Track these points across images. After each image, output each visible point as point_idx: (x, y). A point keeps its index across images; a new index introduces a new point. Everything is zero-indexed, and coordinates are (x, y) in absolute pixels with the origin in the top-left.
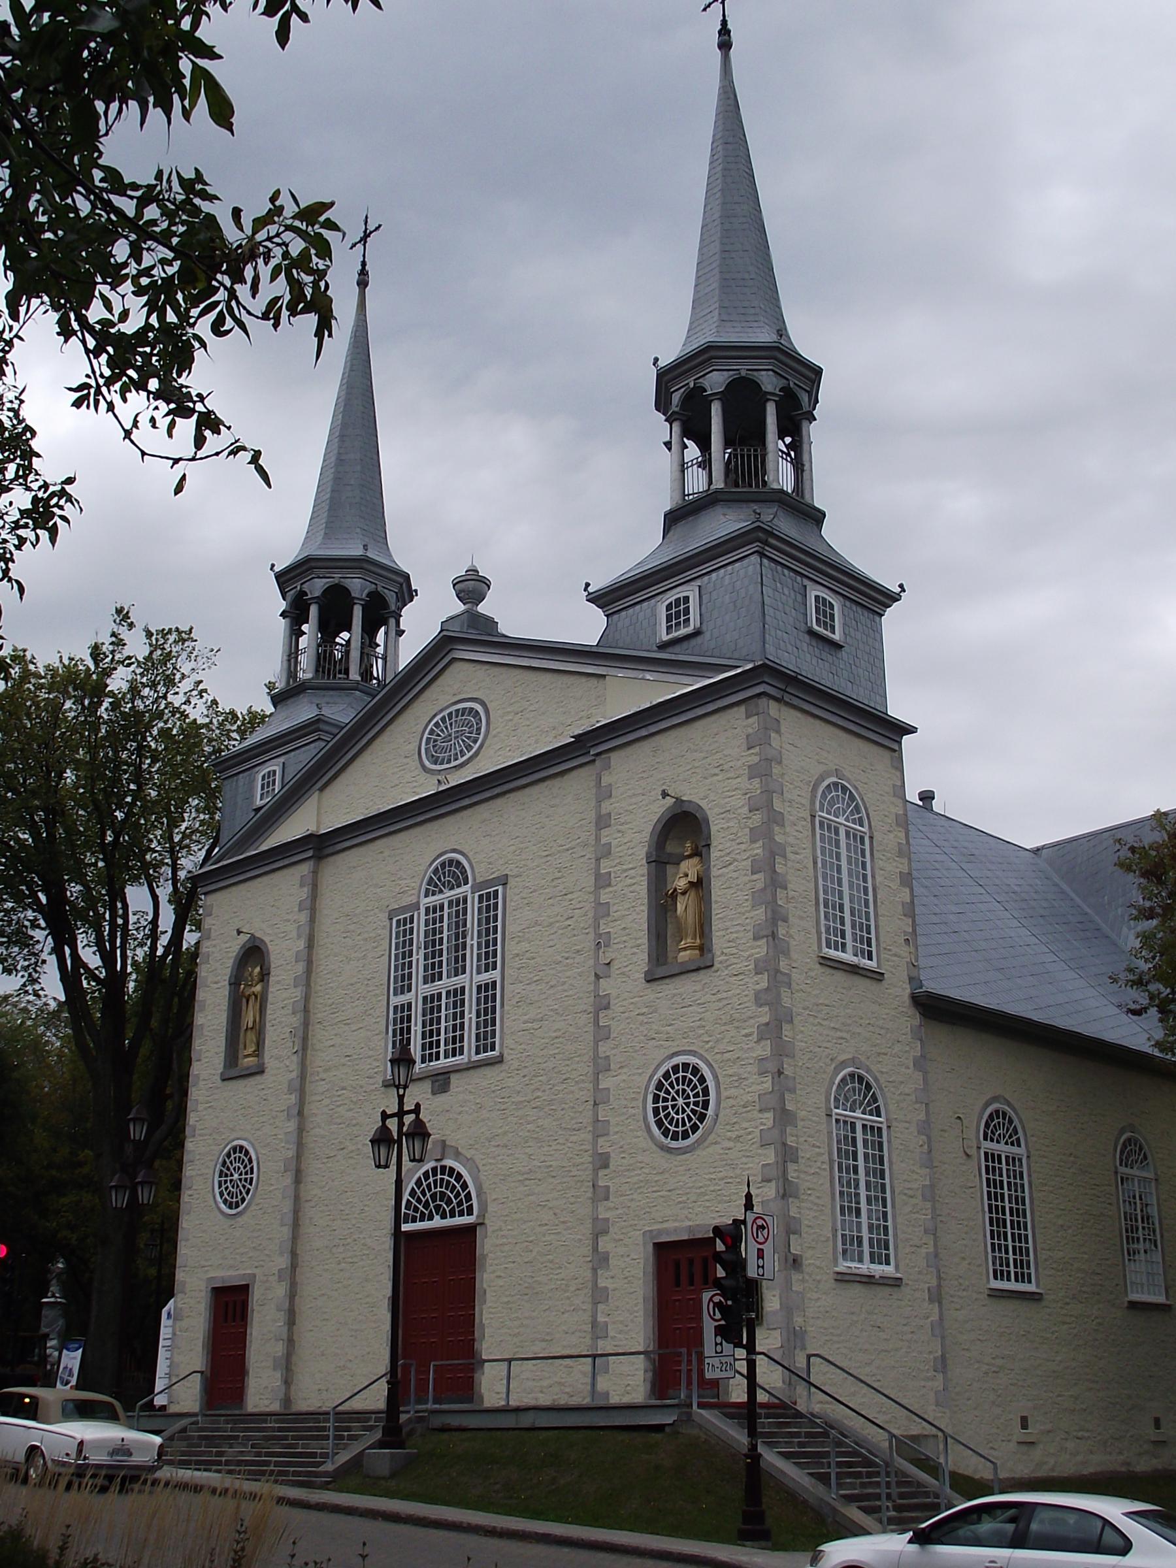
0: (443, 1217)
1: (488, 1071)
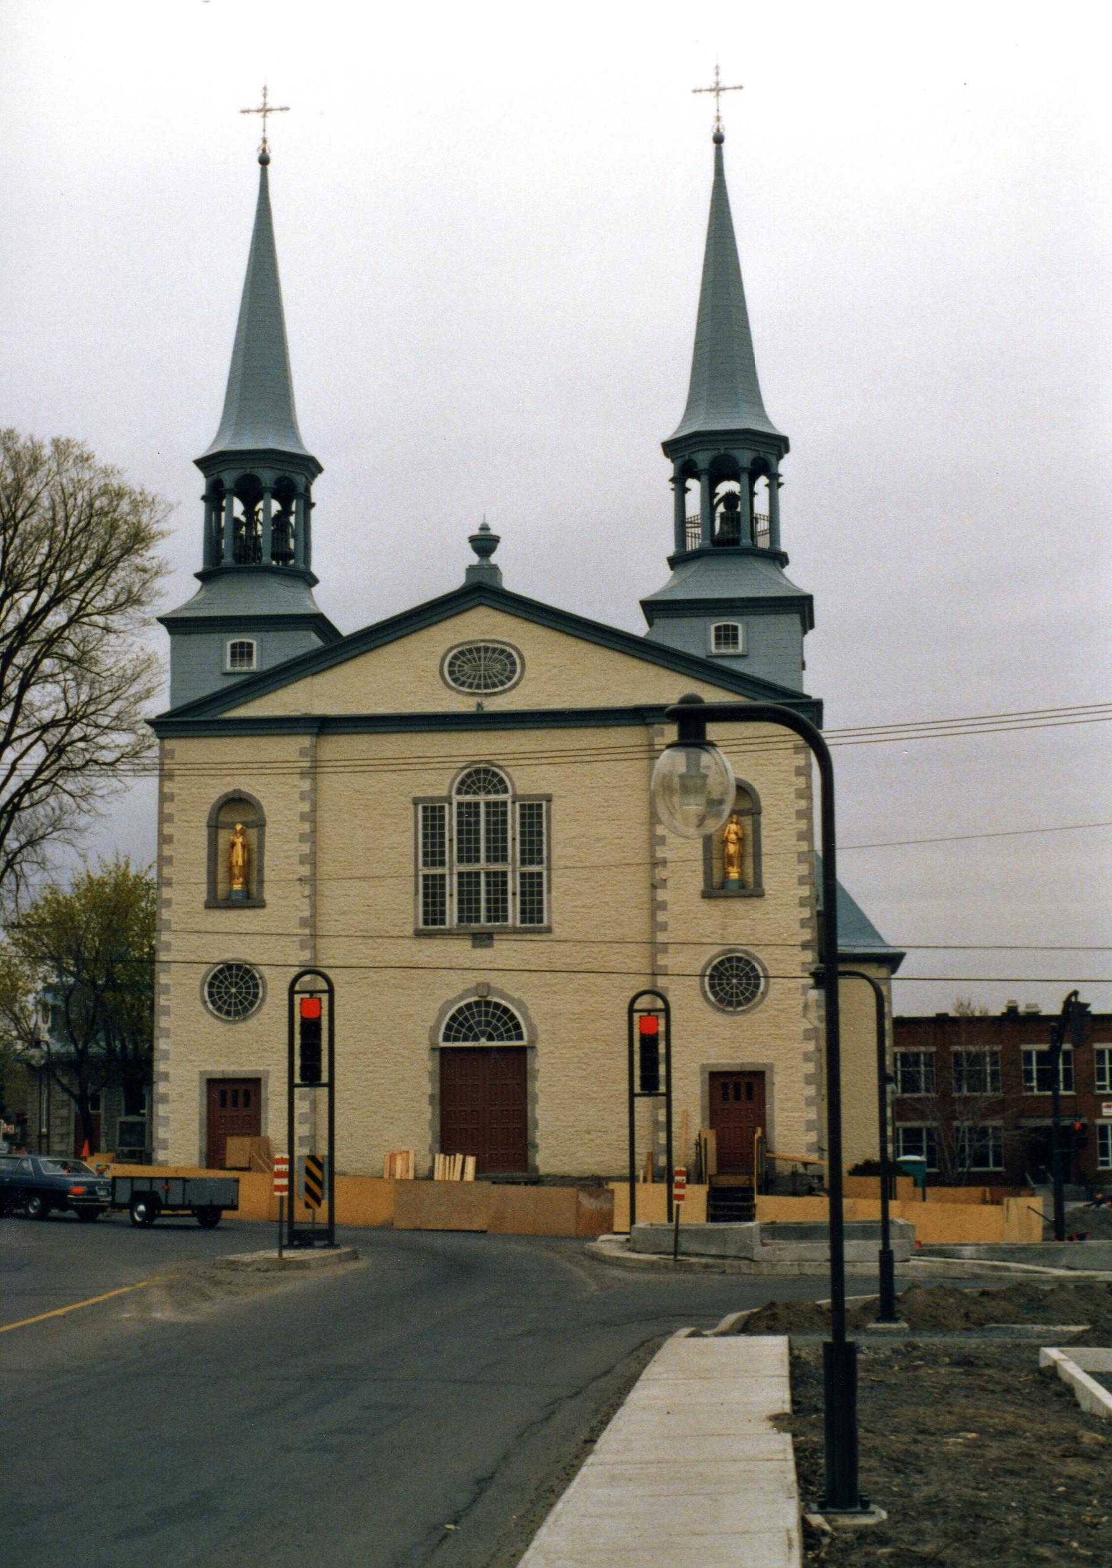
0: (490, 1038)
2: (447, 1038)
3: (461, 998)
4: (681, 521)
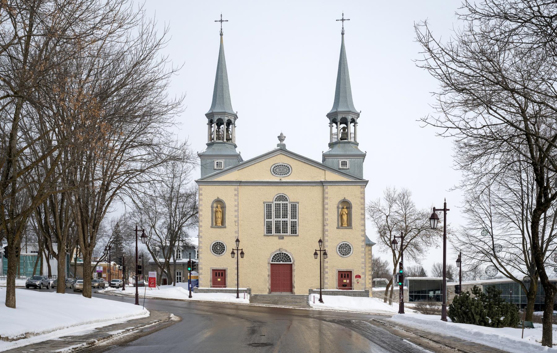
0: (283, 261)
1: (295, 237)
2: (272, 261)
3: (276, 251)
4: (331, 134)
